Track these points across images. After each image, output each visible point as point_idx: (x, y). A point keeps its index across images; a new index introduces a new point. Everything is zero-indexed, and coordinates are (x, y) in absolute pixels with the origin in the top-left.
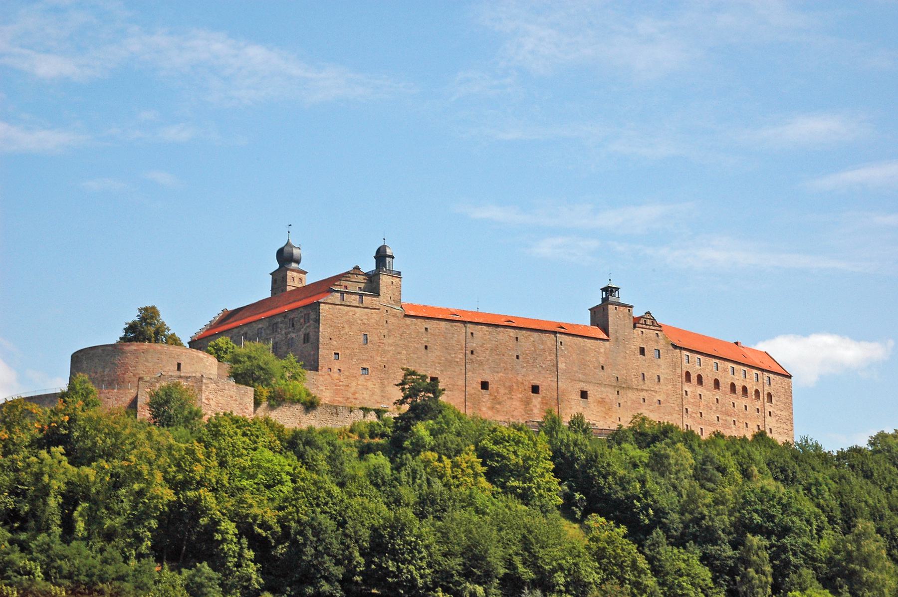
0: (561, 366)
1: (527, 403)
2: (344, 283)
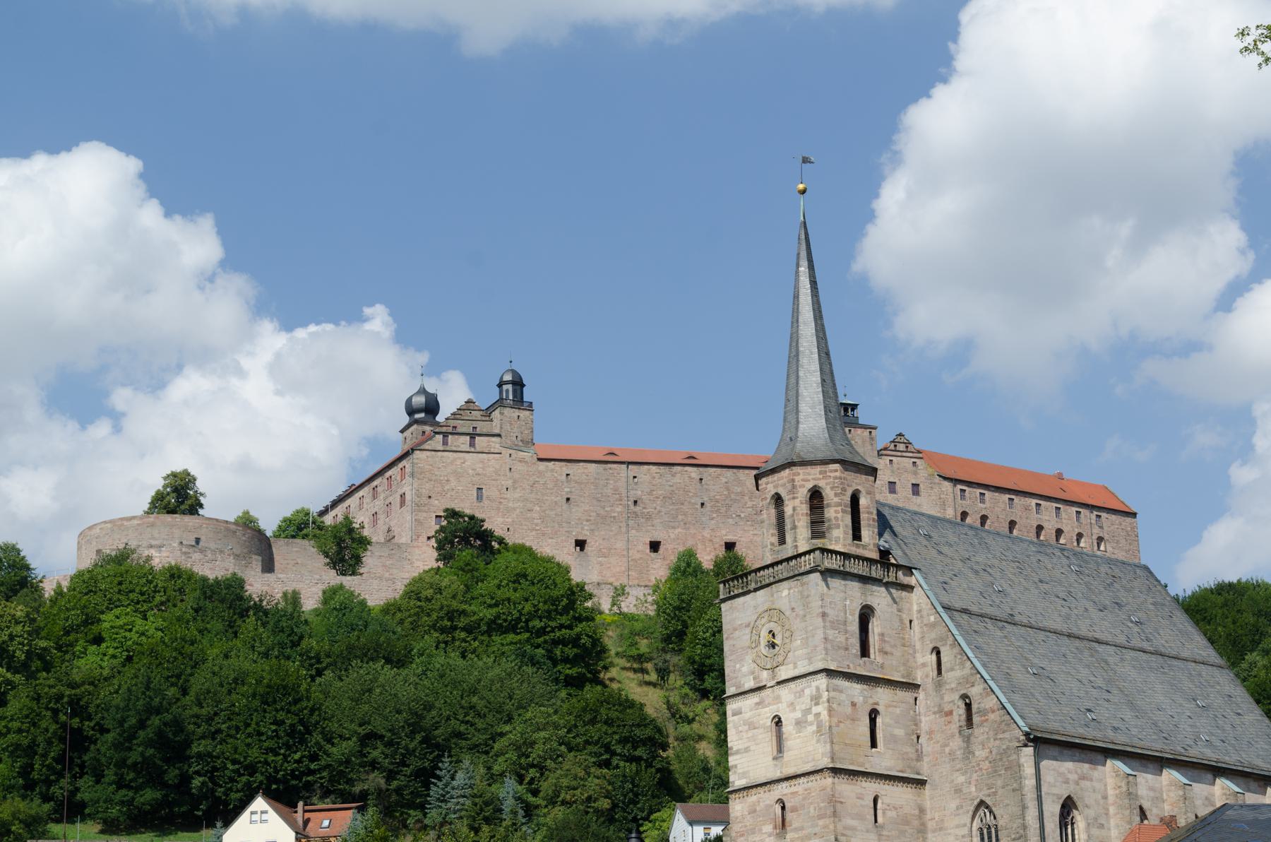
2: (452, 423)
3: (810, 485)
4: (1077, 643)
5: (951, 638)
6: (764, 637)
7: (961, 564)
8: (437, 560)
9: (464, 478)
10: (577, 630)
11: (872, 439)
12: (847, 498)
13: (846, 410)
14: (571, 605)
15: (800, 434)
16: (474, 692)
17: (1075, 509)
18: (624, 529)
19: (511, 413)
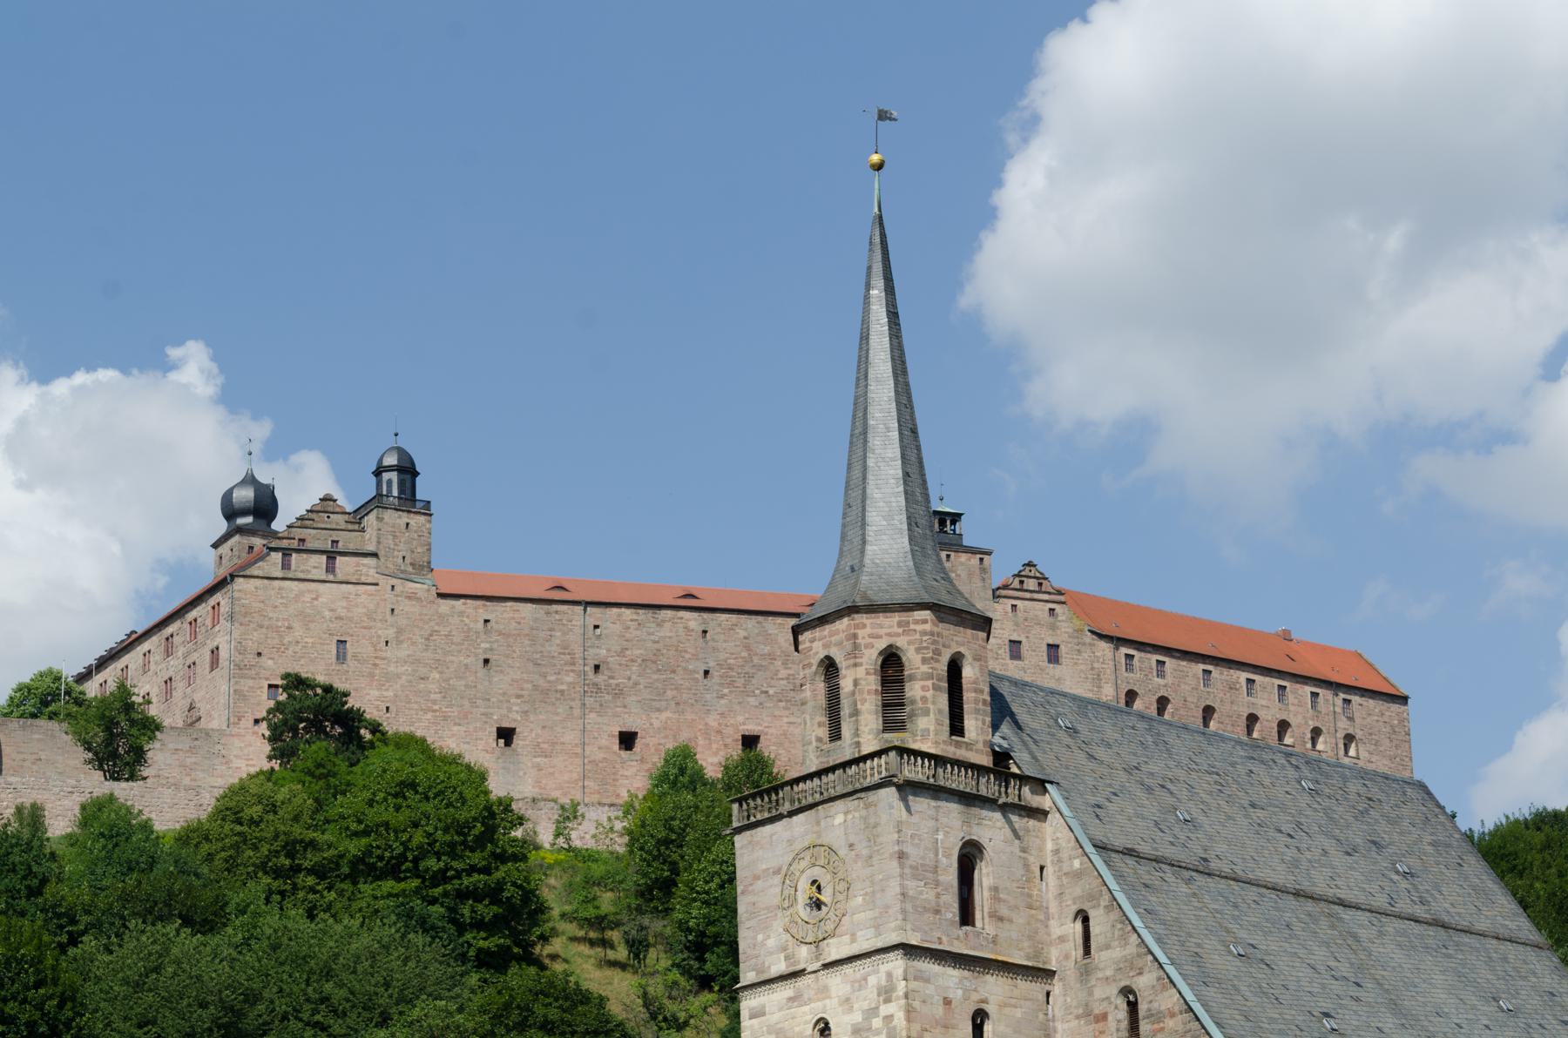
2: (299, 533)
3: (882, 644)
4: (1310, 906)
5: (1107, 897)
6: (804, 891)
7: (1123, 776)
8: (270, 758)
9: (313, 624)
10: (499, 875)
11: (984, 570)
12: (943, 667)
13: (942, 523)
14: (489, 834)
15: (867, 561)
16: (328, 974)
17: (1308, 689)
18: (577, 712)
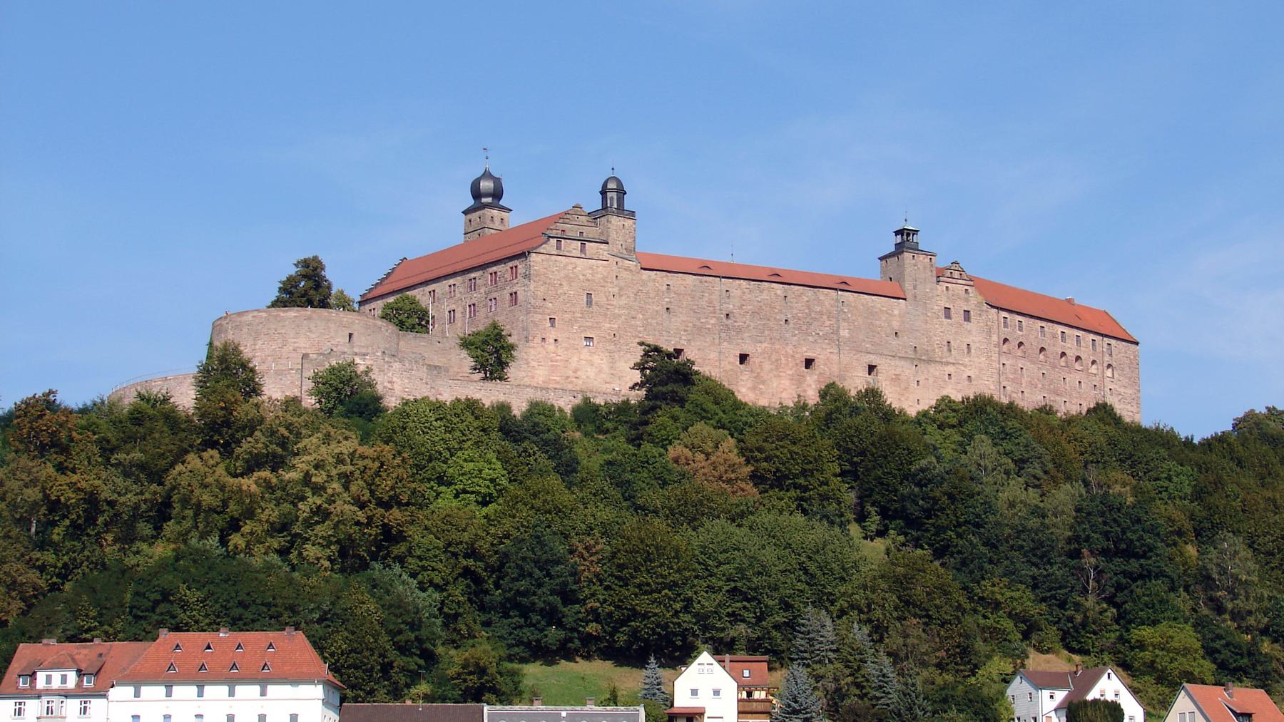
0: (844, 333)
1: (799, 380)
2: (561, 226)
18: (717, 341)
19: (616, 221)
